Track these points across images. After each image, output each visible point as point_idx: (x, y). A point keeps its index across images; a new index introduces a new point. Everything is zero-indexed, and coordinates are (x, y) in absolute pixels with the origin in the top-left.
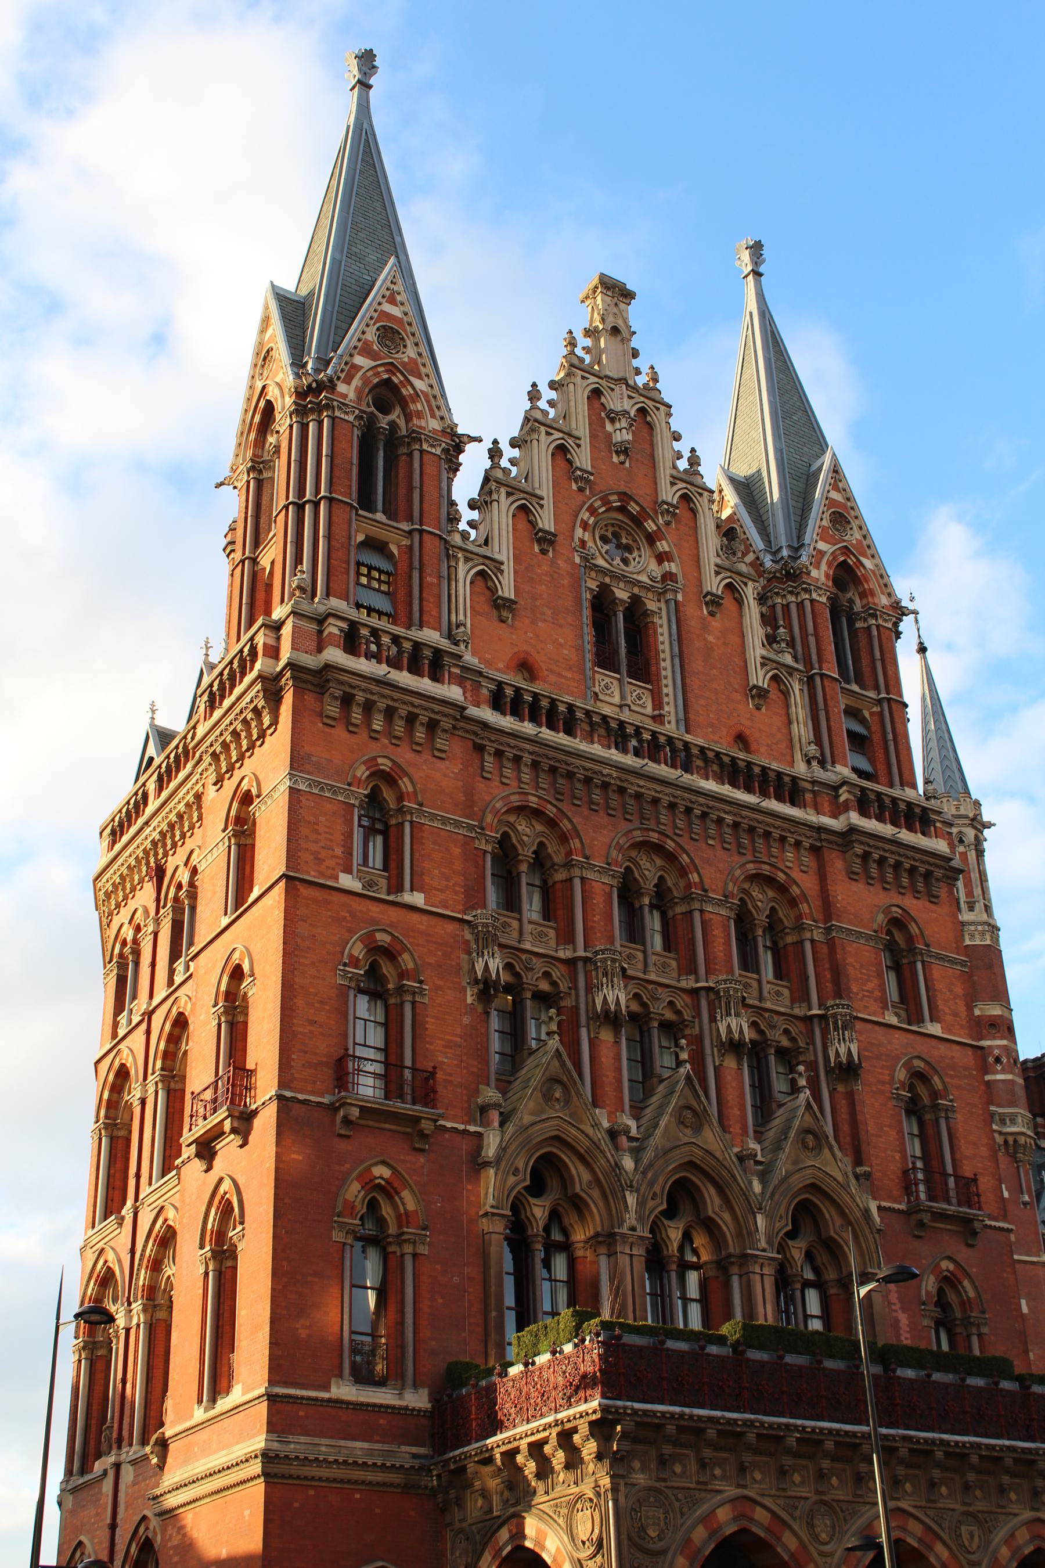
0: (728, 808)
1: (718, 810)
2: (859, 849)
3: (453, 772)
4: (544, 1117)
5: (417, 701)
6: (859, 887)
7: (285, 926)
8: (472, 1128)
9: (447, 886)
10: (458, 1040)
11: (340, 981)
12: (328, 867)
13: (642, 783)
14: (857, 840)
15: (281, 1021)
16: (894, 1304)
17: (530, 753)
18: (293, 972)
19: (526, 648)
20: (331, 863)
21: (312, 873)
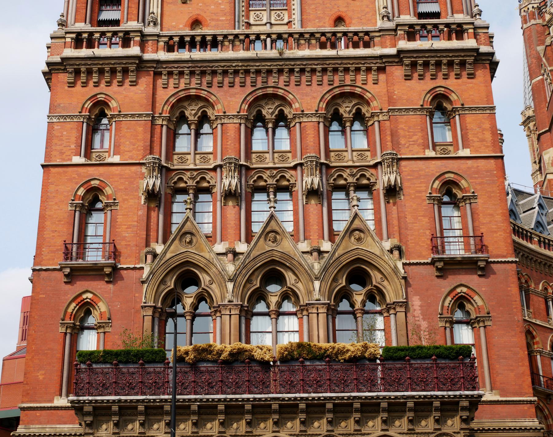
0: (316, 62)
1: (311, 65)
2: (407, 61)
3: (141, 90)
4: (178, 253)
5: (113, 62)
6: (414, 83)
7: (42, 189)
8: (138, 266)
9: (133, 149)
10: (136, 223)
11: (70, 208)
12: (67, 156)
13: (258, 64)
14: (404, 57)
15: (38, 234)
16: (418, 317)
17: (188, 68)
18: (45, 210)
19: (197, 12)
20: (69, 153)
21: (58, 160)
